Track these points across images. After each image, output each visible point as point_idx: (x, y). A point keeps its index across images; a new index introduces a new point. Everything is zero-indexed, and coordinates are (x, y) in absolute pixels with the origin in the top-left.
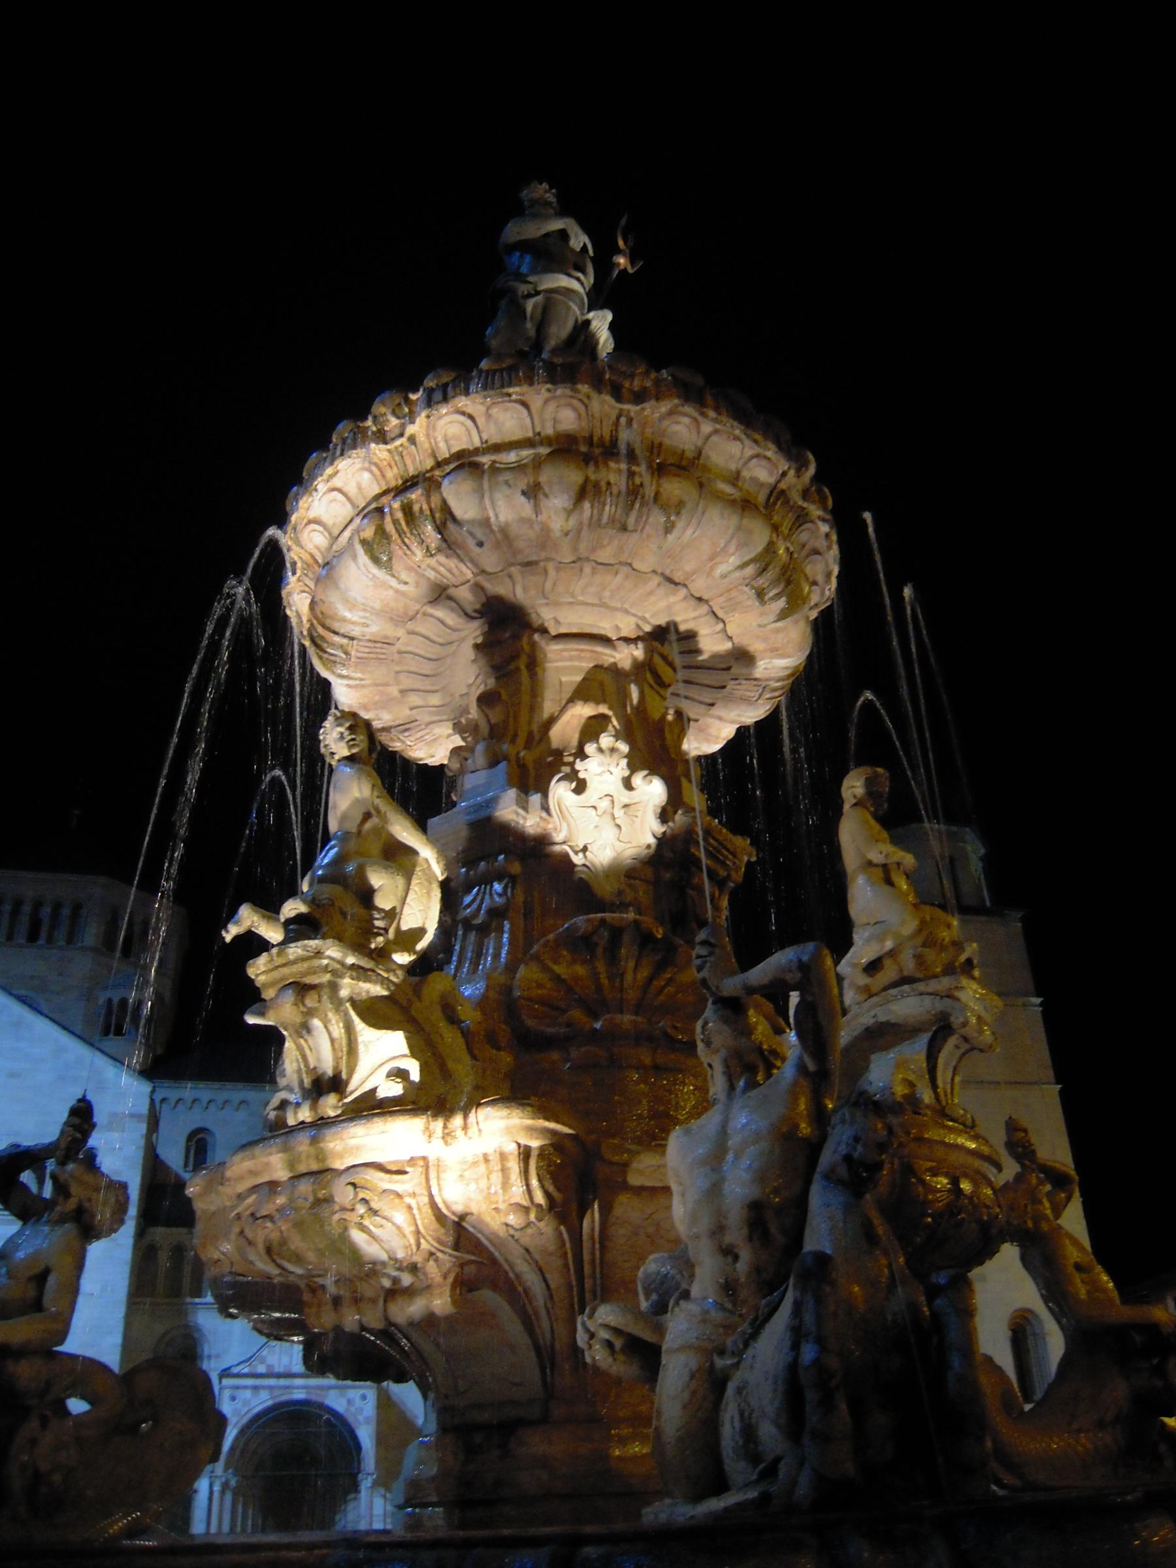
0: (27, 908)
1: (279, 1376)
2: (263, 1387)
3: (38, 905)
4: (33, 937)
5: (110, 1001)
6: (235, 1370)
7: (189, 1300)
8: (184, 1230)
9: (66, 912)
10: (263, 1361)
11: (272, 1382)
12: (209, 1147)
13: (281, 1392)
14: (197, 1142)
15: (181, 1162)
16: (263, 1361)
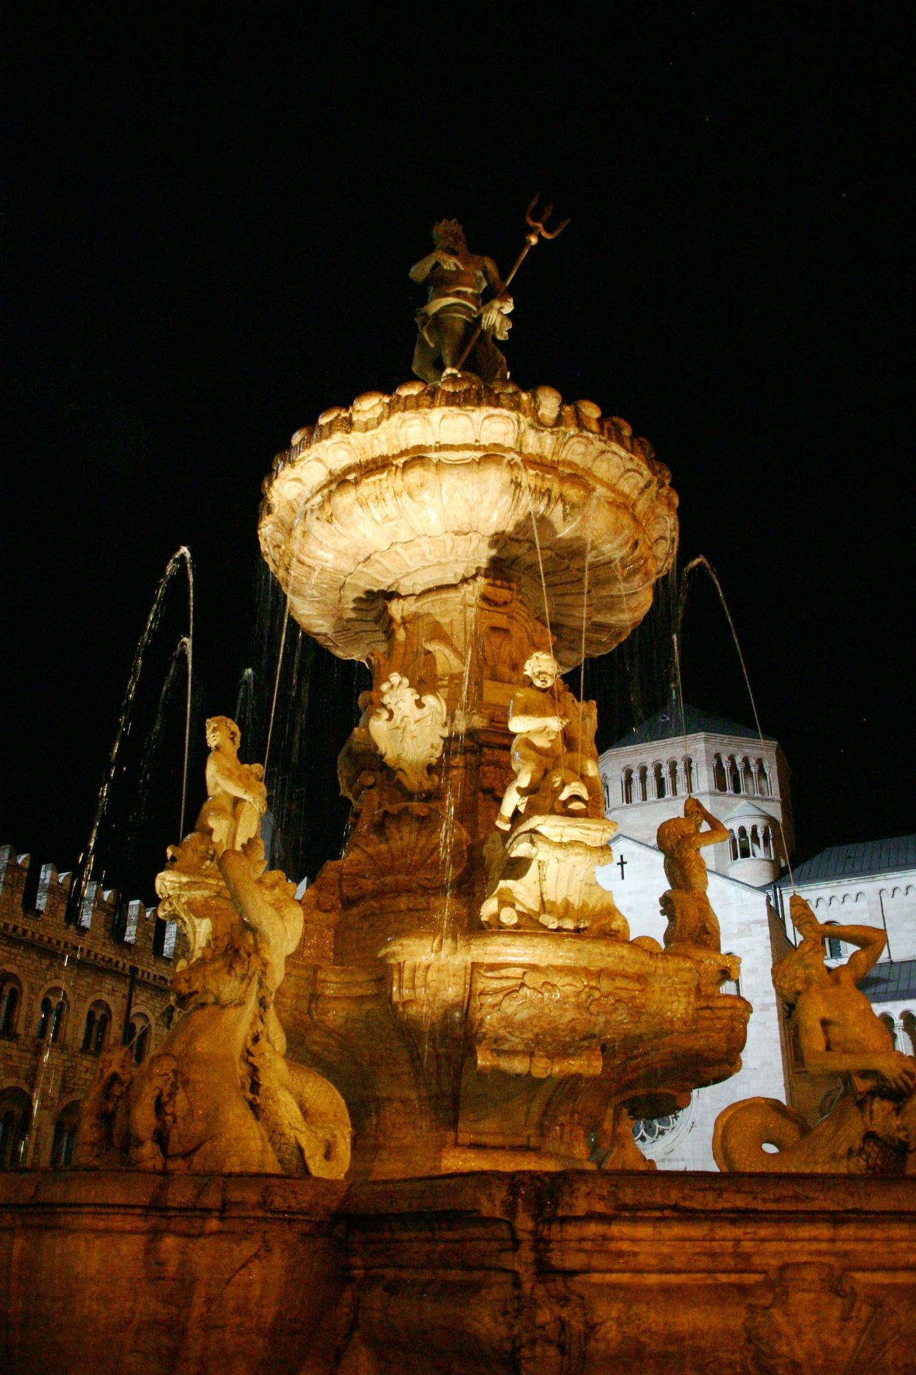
0: (650, 772)
3: (658, 768)
4: (661, 793)
9: (680, 767)
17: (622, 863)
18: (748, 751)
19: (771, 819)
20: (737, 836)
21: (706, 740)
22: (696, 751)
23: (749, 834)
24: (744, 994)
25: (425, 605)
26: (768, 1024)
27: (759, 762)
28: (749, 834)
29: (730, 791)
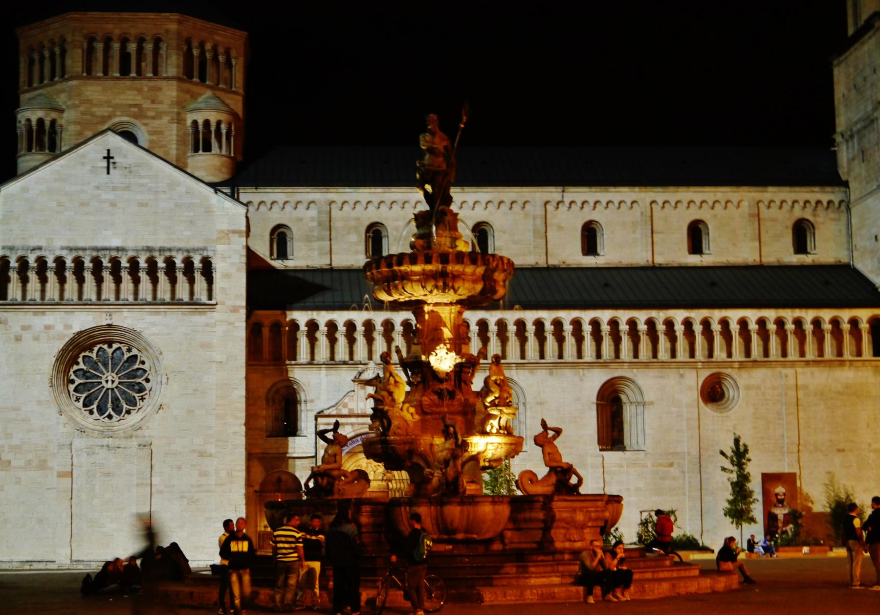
0: (116, 46)
1: (358, 416)
2: (347, 424)
3: (124, 41)
4: (125, 71)
5: (195, 123)
6: (326, 412)
7: (288, 362)
8: (279, 312)
10: (345, 406)
11: (353, 420)
12: (288, 239)
13: (360, 426)
14: (278, 235)
15: (268, 253)
16: (345, 406)
17: (108, 158)
18: (218, 38)
19: (233, 114)
20: (201, 128)
21: (179, 22)
22: (167, 31)
23: (213, 128)
24: (540, 449)
25: (436, 309)
26: (237, 324)
27: (227, 53)
28: (213, 128)
29: (195, 80)
